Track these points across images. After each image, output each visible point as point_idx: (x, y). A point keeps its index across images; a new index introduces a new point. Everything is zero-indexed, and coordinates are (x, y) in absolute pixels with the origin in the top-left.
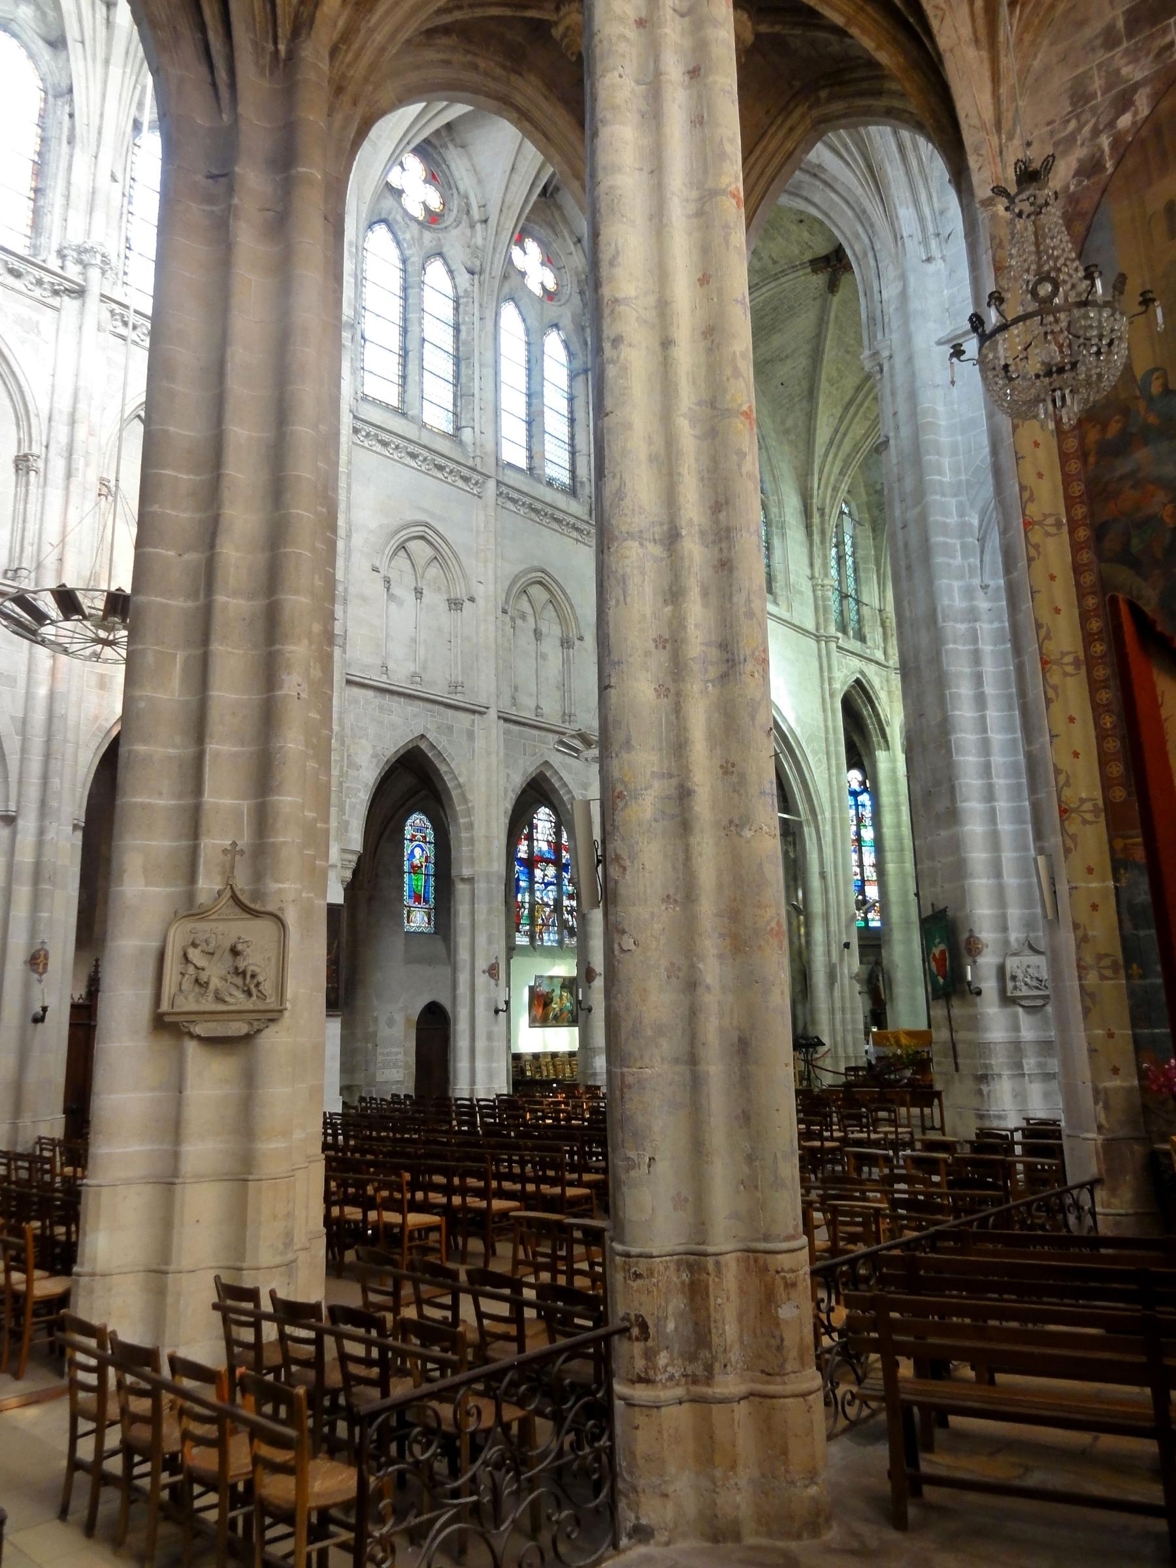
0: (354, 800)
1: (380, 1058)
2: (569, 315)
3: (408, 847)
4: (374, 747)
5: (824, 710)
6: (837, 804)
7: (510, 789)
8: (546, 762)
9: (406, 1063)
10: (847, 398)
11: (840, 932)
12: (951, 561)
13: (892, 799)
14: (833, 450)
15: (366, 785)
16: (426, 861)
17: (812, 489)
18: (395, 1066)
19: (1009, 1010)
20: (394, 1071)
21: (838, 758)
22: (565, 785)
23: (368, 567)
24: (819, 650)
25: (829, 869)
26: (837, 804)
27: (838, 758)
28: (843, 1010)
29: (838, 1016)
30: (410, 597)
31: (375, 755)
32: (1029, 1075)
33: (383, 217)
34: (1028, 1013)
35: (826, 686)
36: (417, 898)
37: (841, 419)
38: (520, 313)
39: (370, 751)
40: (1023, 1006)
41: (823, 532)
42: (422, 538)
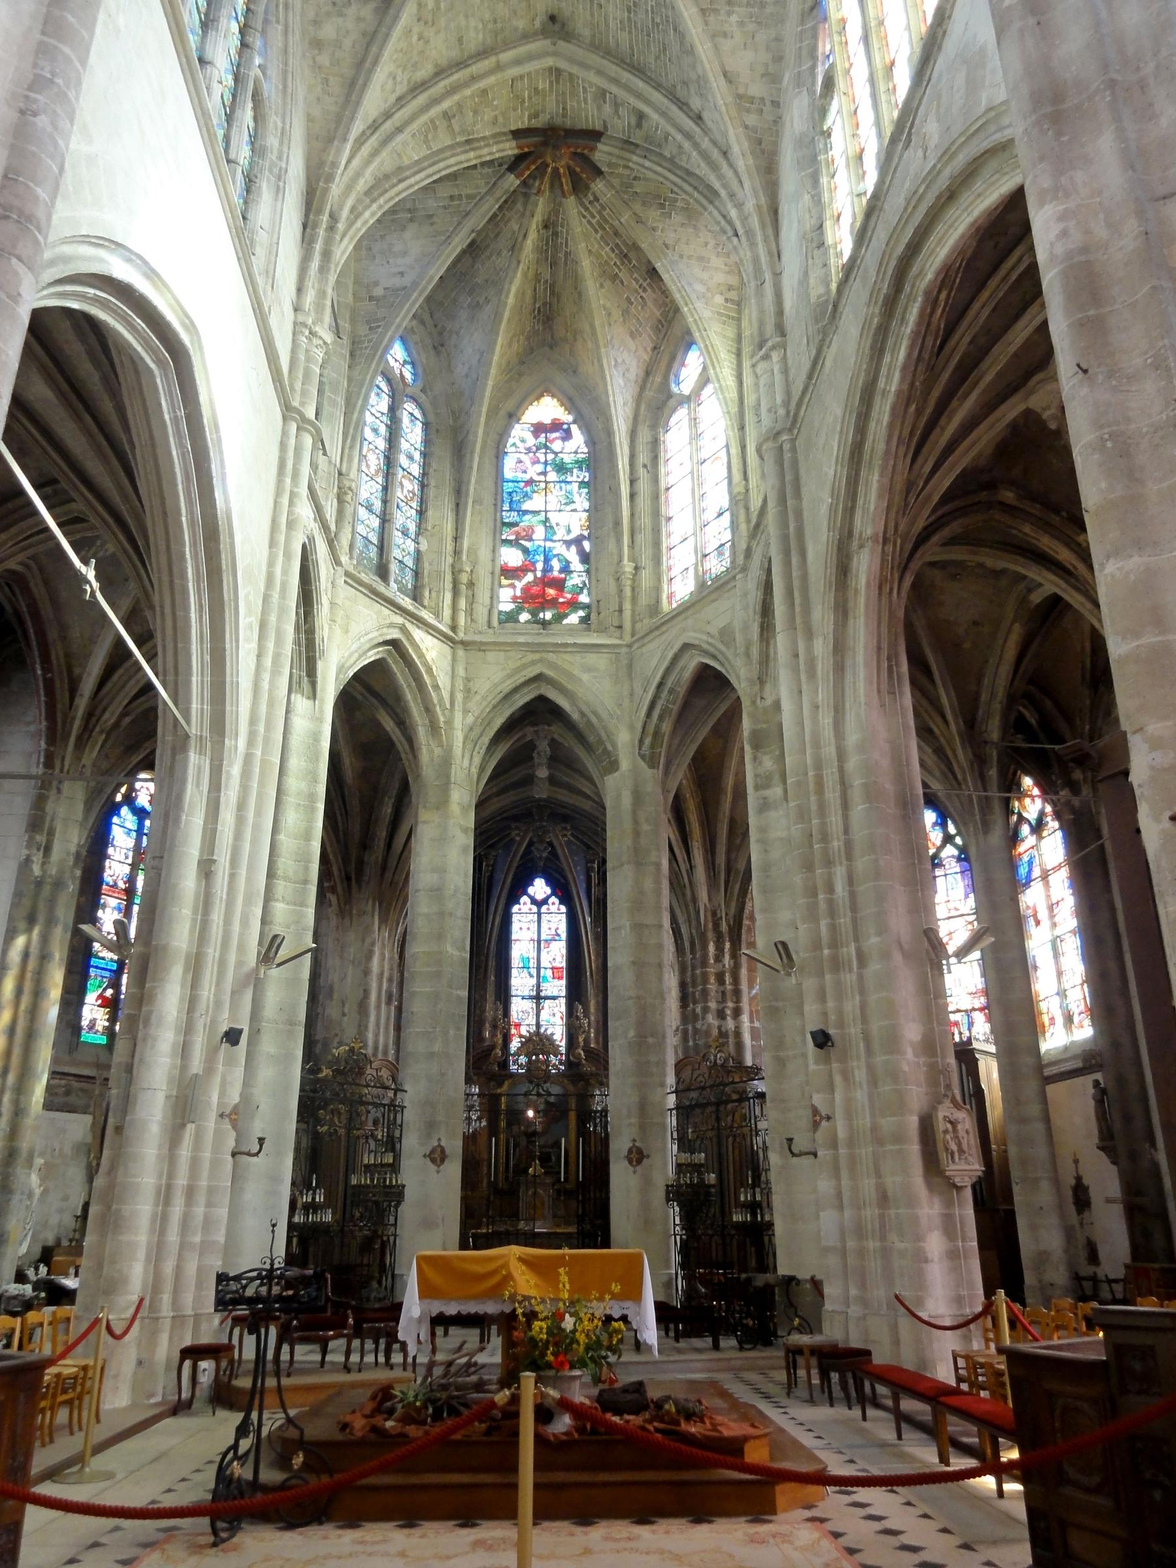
5: (272, 543)
6: (261, 729)
10: (422, 74)
11: (218, 1004)
13: (303, 785)
14: (373, 141)
17: (334, 165)
21: (279, 642)
24: (285, 433)
25: (223, 858)
26: (261, 729)
27: (279, 642)
28: (190, 1192)
29: (177, 1210)
35: (285, 501)
37: (401, 101)
41: (327, 255)
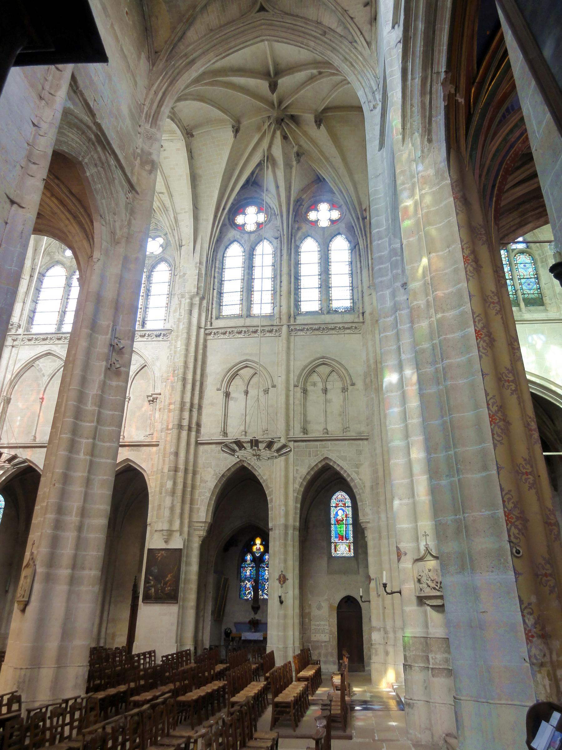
0: (203, 497)
1: (313, 627)
2: (344, 225)
3: (333, 511)
4: (215, 470)
7: (298, 476)
8: (326, 458)
9: (331, 631)
12: (385, 278)
15: (210, 489)
16: (346, 516)
18: (323, 632)
19: (421, 609)
20: (322, 635)
22: (342, 468)
23: (216, 388)
30: (243, 396)
31: (215, 474)
32: (432, 669)
33: (232, 239)
34: (438, 611)
36: (341, 538)
38: (315, 239)
39: (213, 473)
40: (432, 606)
42: (247, 367)
